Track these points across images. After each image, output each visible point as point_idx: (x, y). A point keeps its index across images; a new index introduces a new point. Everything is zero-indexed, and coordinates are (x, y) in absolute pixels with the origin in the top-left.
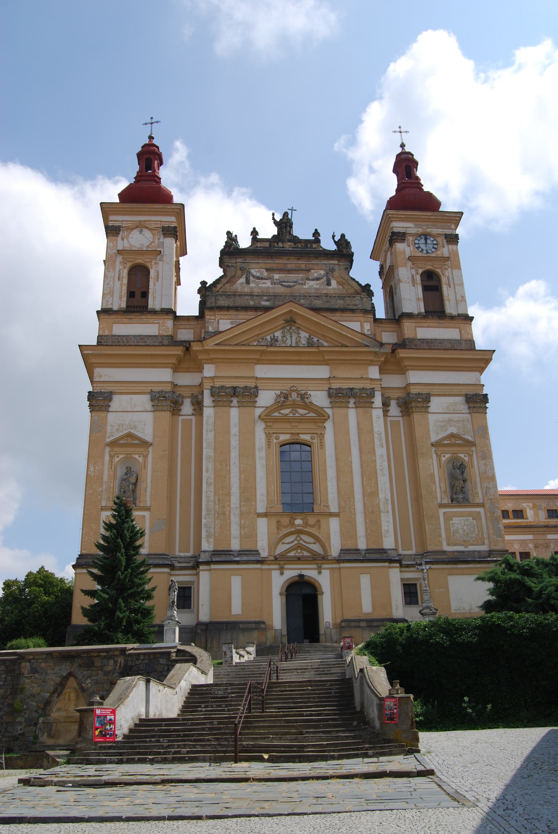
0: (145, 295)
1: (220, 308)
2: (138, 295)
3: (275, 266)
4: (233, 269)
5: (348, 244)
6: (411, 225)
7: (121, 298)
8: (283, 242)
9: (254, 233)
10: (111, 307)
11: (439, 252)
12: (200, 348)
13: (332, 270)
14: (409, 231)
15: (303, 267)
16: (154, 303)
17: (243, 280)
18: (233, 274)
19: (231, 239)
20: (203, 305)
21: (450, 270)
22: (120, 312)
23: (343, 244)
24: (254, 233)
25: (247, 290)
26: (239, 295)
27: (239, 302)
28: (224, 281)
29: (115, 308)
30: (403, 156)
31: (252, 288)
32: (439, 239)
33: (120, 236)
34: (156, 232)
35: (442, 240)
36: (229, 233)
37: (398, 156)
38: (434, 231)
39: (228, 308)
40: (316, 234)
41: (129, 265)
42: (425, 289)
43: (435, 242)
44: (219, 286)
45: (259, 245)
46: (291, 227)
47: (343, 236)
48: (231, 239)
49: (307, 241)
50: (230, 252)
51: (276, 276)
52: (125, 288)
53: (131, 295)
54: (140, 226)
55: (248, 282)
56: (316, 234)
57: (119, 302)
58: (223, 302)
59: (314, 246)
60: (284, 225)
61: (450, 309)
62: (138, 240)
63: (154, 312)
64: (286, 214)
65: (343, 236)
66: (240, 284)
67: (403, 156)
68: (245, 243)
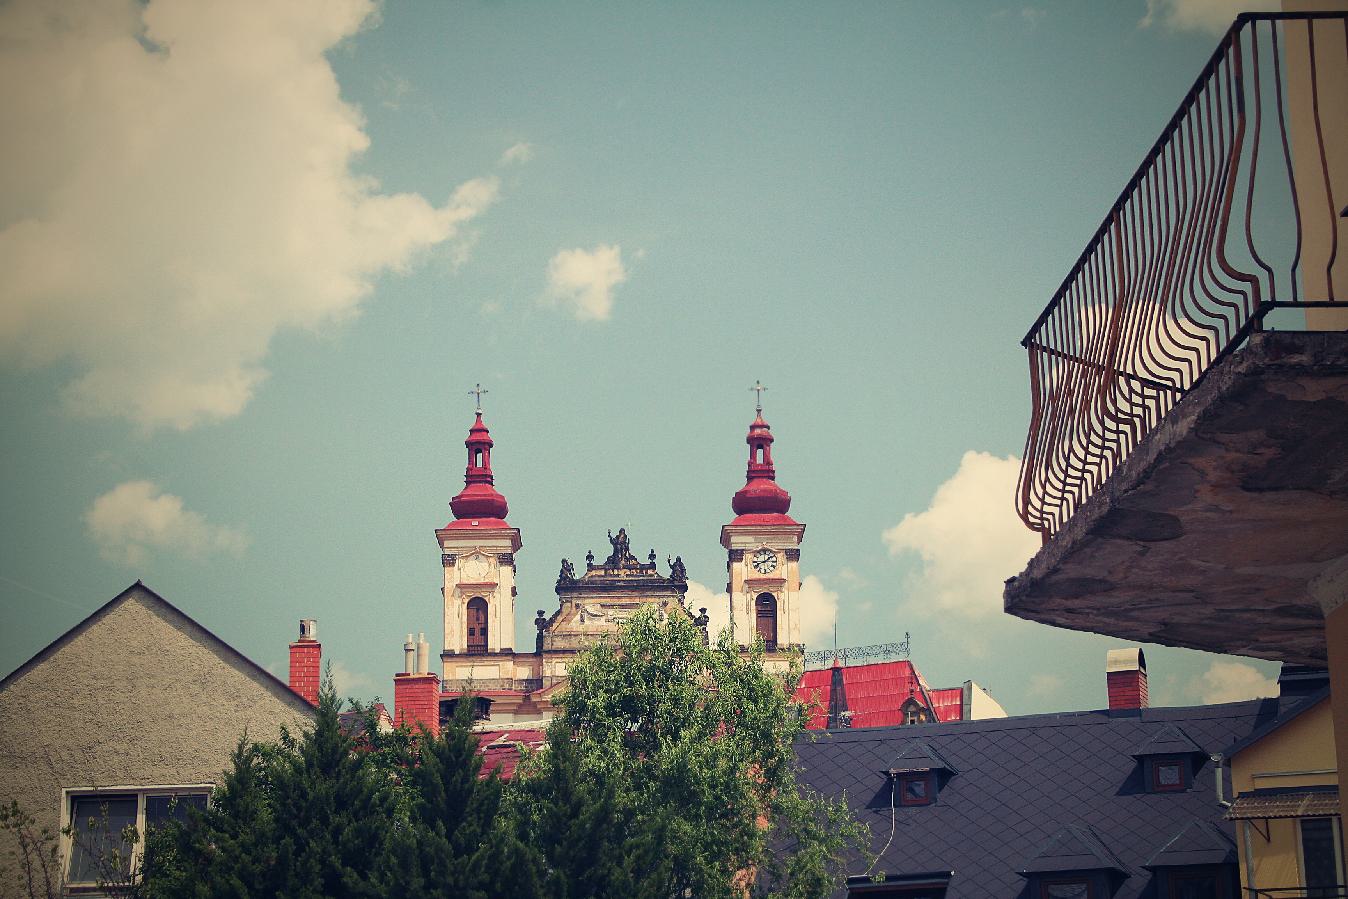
0: (484, 631)
1: (556, 652)
2: (477, 632)
3: (608, 601)
4: (569, 604)
5: (683, 570)
6: (750, 539)
7: (461, 637)
8: (618, 569)
9: (590, 557)
10: (452, 648)
11: (778, 572)
12: (538, 700)
13: (665, 604)
14: (748, 547)
15: (637, 601)
16: (495, 643)
17: (578, 617)
18: (567, 612)
19: (567, 567)
20: (540, 639)
21: (786, 592)
22: (460, 655)
23: (678, 567)
24: (590, 557)
25: (581, 629)
26: (575, 635)
27: (574, 643)
28: (560, 618)
29: (457, 652)
30: (758, 431)
31: (587, 627)
32: (779, 555)
33: (456, 565)
34: (491, 560)
35: (781, 557)
36: (564, 561)
37: (753, 428)
38: (774, 546)
39: (564, 651)
40: (652, 556)
41: (467, 601)
42: (760, 614)
43: (774, 559)
44: (555, 625)
45: (594, 573)
46: (627, 549)
47: (679, 559)
48: (567, 567)
49: (643, 567)
50: (567, 586)
51: (611, 612)
52: (465, 626)
53: (471, 632)
54: (476, 554)
55: (582, 621)
56: (652, 556)
57: (458, 642)
58: (560, 644)
59: (650, 572)
60: (620, 543)
61: (783, 640)
62: (473, 571)
63: (495, 655)
64: (622, 531)
65: (679, 559)
66: (575, 624)
67: (758, 431)
68: (579, 572)
